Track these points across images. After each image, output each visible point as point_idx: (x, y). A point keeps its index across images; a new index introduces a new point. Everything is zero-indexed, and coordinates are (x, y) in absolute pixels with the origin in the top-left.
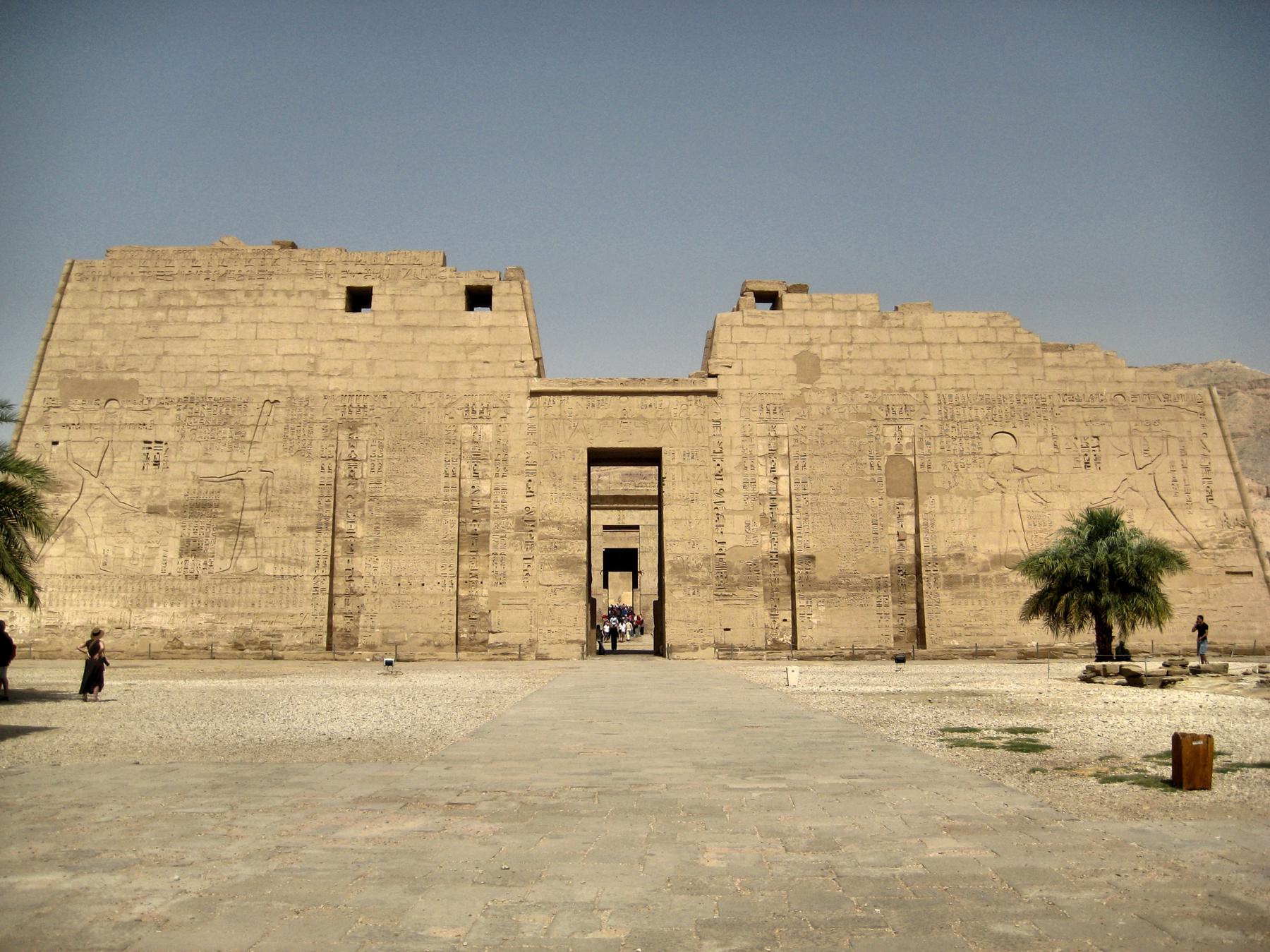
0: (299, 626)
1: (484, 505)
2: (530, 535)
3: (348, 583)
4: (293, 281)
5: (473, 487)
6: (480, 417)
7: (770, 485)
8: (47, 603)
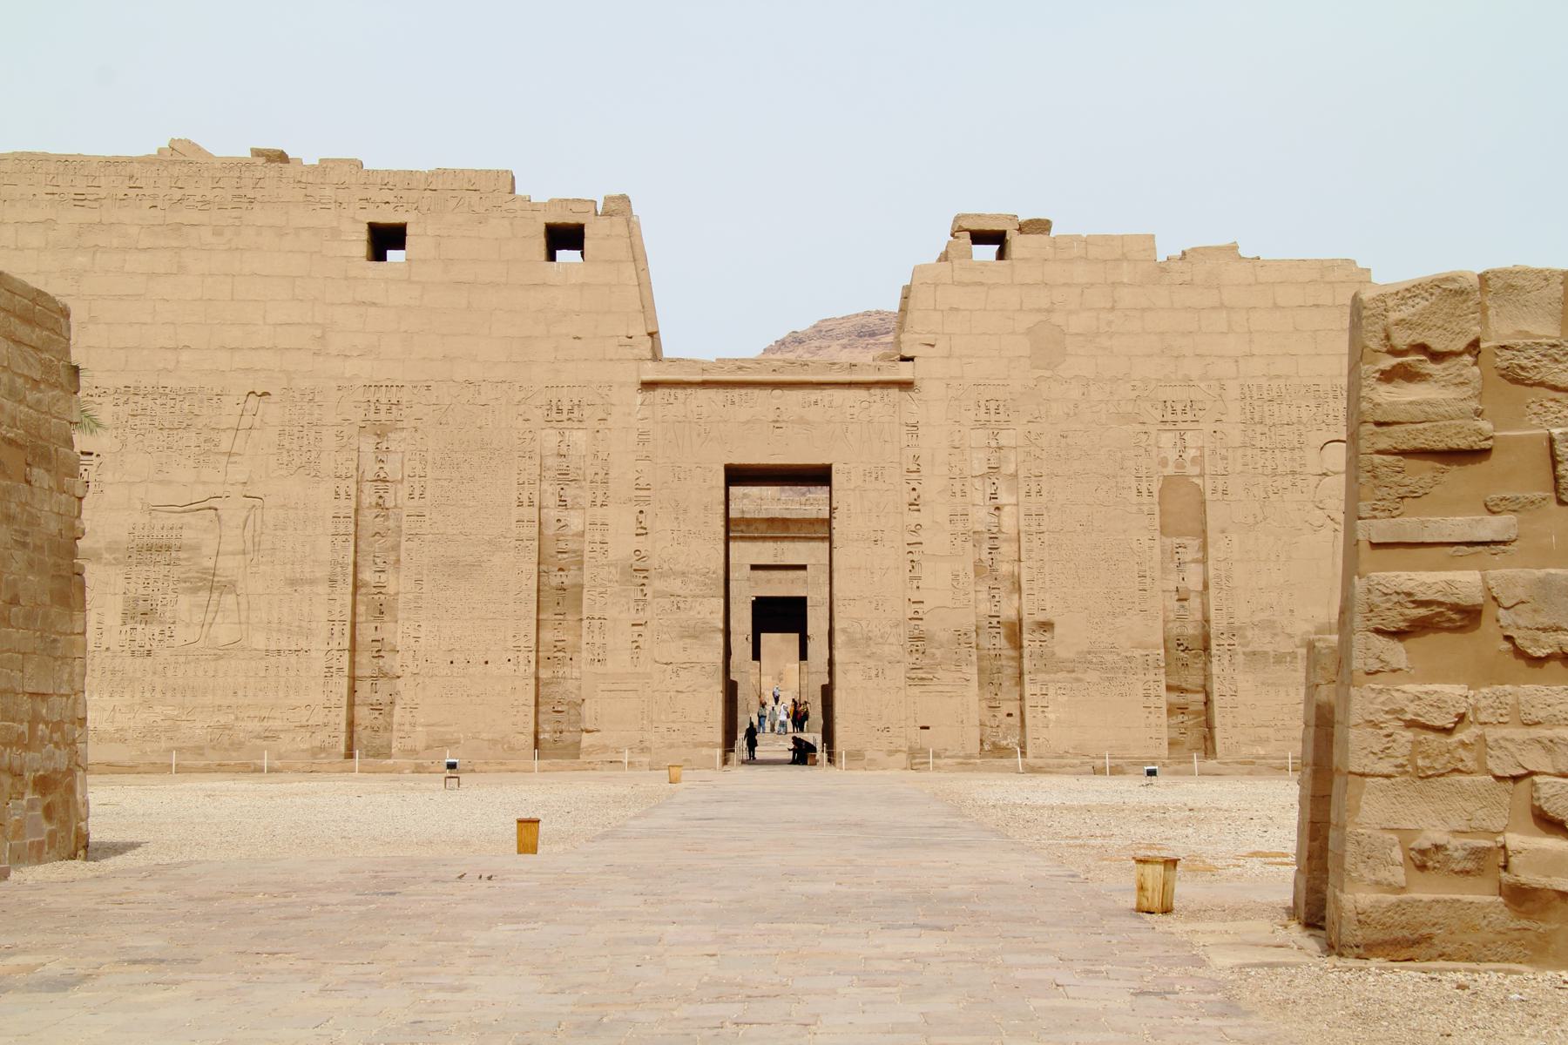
1: (572, 546)
2: (642, 590)
3: (375, 660)
4: (286, 213)
5: (559, 520)
6: (569, 419)
7: (989, 519)
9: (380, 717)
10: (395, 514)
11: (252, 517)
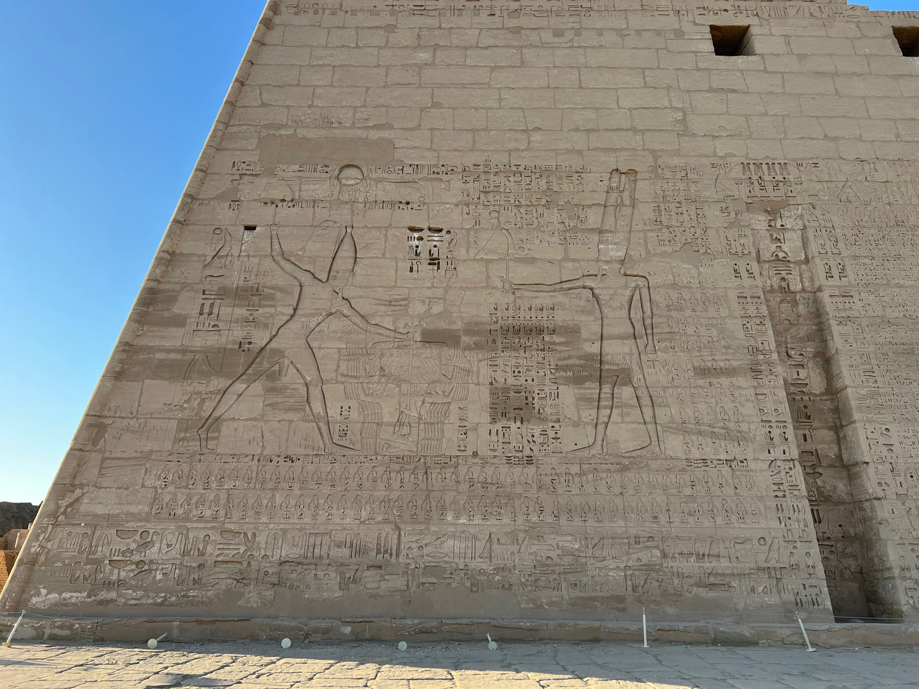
8: (222, 513)
9: (832, 557)
10: (804, 299)
11: (636, 297)
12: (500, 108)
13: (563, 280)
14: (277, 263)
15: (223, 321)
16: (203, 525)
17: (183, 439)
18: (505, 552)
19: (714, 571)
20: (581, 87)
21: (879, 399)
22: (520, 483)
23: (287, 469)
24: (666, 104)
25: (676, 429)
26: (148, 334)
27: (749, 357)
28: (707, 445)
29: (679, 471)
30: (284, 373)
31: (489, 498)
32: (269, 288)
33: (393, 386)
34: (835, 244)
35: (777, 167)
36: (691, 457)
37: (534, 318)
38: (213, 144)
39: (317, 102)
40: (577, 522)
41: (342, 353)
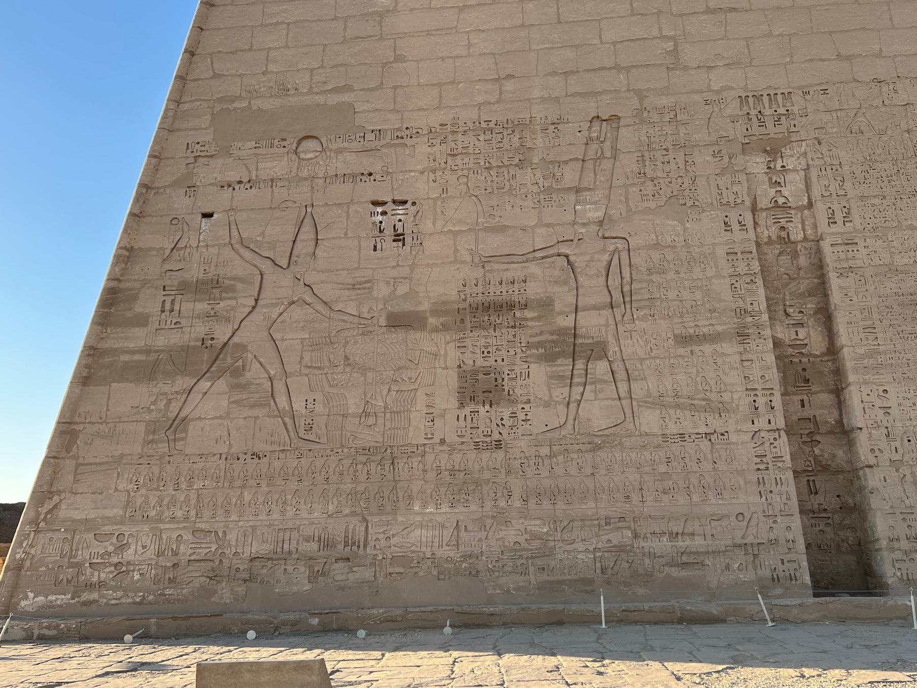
0: (739, 541)
8: (193, 513)
9: (828, 529)
10: (806, 249)
11: (615, 261)
12: (469, 55)
13: (536, 248)
14: (236, 252)
15: (184, 317)
16: (175, 526)
17: (152, 442)
18: (472, 539)
19: (688, 550)
20: (560, 22)
21: (878, 357)
22: (488, 469)
23: (254, 466)
24: (655, 33)
25: (653, 403)
26: (112, 335)
27: (736, 320)
28: (686, 419)
29: (654, 447)
30: (247, 368)
31: (456, 485)
32: (228, 279)
33: (359, 375)
34: (841, 184)
35: (780, 97)
36: (668, 432)
37: (504, 293)
38: (165, 126)
39: (271, 67)
40: (547, 505)
41: (305, 344)
